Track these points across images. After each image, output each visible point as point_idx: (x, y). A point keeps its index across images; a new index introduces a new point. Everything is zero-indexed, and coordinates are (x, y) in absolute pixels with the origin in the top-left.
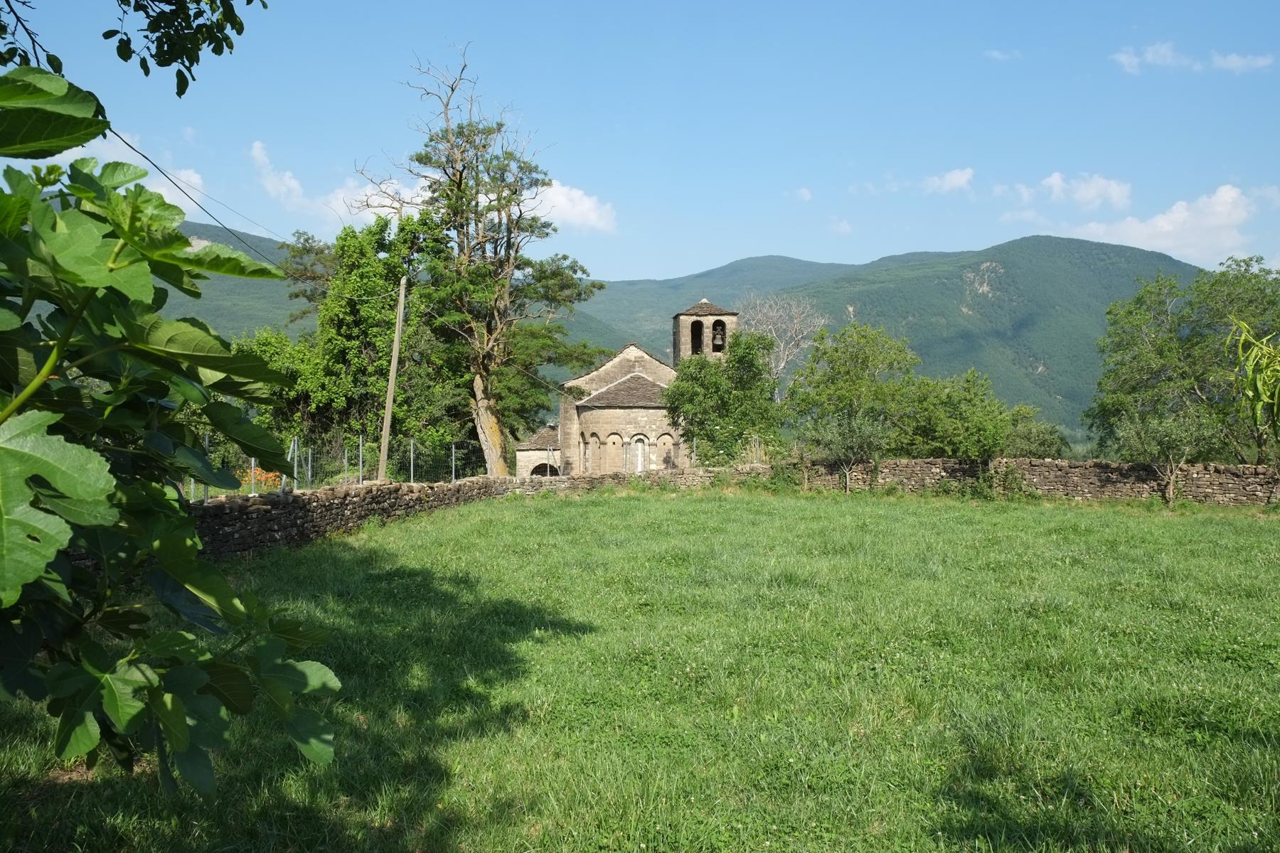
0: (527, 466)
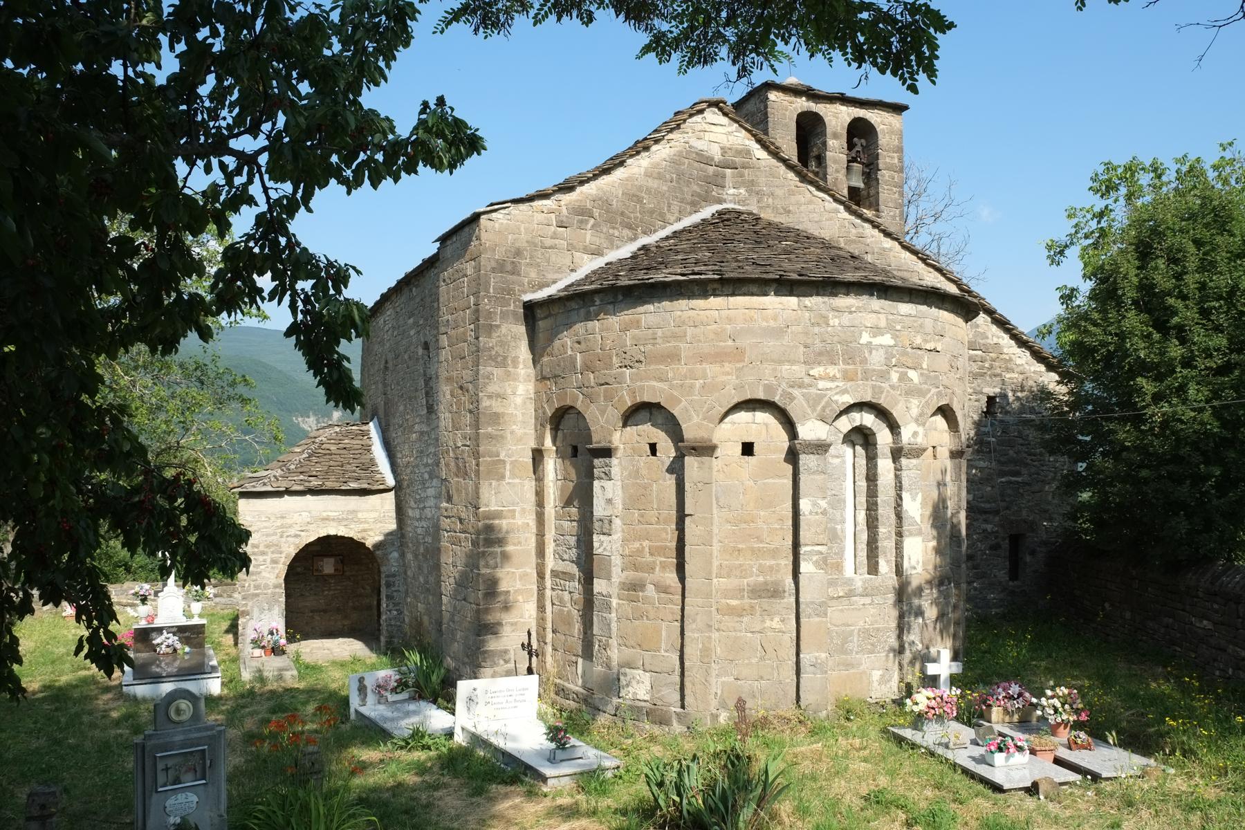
0: (277, 548)
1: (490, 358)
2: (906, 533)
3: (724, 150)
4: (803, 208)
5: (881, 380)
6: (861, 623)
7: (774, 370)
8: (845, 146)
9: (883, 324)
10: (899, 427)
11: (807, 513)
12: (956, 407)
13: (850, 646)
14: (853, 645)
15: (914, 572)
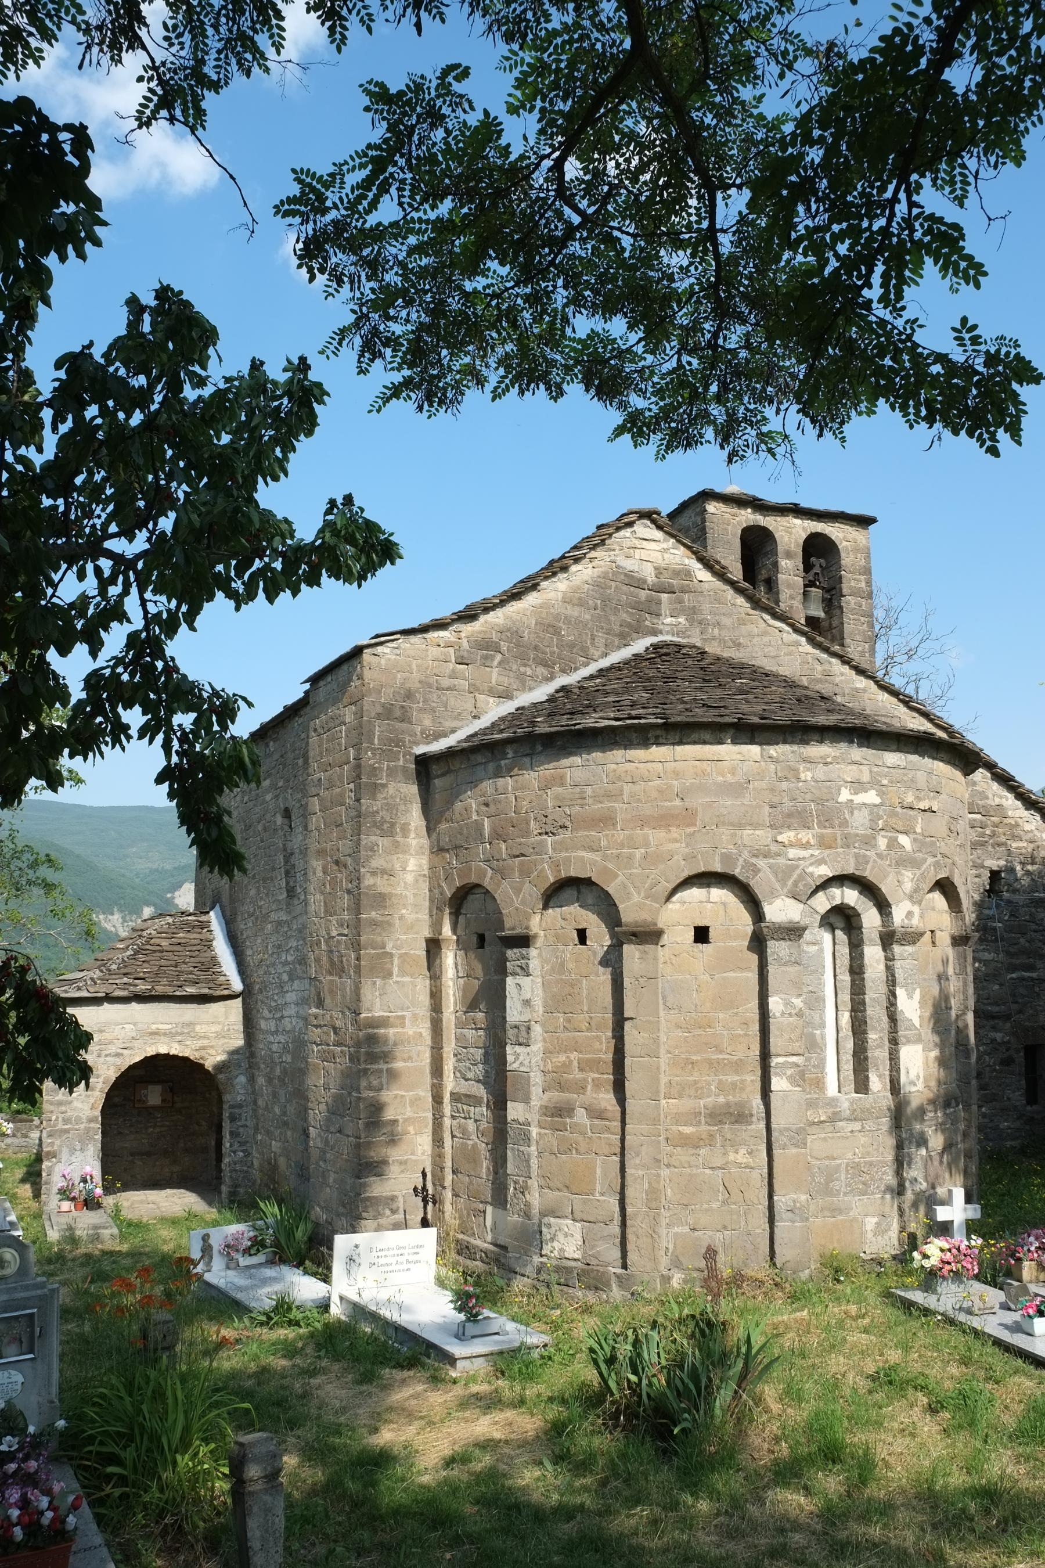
1: (375, 824)
2: (902, 1040)
3: (659, 571)
4: (755, 641)
5: (866, 847)
6: (850, 1155)
7: (734, 835)
8: (801, 567)
9: (866, 777)
10: (889, 905)
11: (778, 1015)
12: (957, 881)
13: (836, 1185)
14: (841, 1183)
15: (913, 1089)
